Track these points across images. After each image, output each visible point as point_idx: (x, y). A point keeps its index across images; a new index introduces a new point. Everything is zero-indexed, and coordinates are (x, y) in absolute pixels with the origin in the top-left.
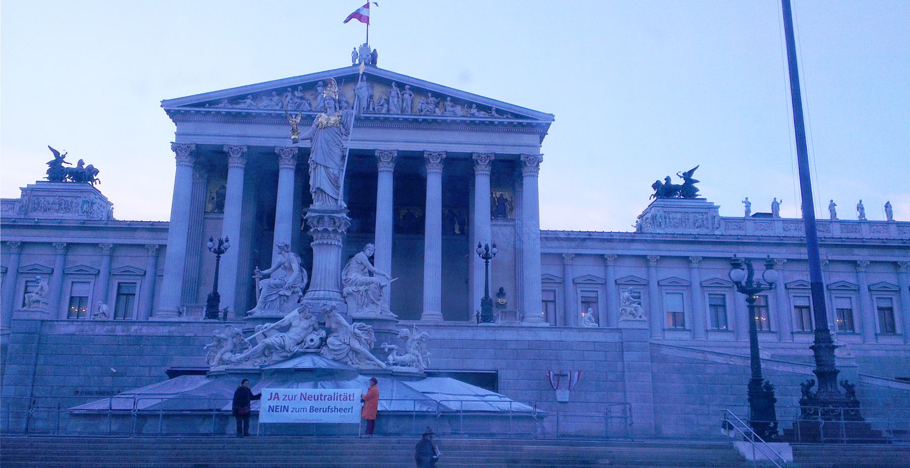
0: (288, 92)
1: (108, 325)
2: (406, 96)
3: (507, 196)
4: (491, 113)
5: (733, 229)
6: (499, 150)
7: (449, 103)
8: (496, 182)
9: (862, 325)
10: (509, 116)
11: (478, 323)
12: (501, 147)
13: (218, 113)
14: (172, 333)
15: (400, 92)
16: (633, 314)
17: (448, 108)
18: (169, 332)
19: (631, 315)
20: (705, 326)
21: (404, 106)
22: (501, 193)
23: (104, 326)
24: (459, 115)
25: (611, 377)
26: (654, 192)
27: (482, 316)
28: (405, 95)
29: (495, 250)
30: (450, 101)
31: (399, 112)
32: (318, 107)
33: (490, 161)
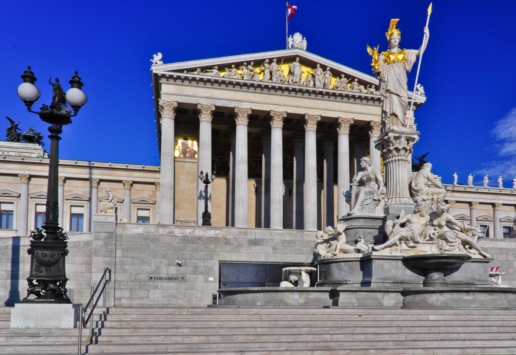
0: (244, 65)
1: (169, 228)
2: (327, 75)
7: (356, 83)
13: (194, 79)
14: (217, 235)
15: (324, 71)
17: (355, 87)
18: (215, 234)
21: (326, 83)
23: (166, 229)
24: (363, 92)
28: (326, 74)
30: (357, 82)
31: (322, 87)
32: (265, 80)
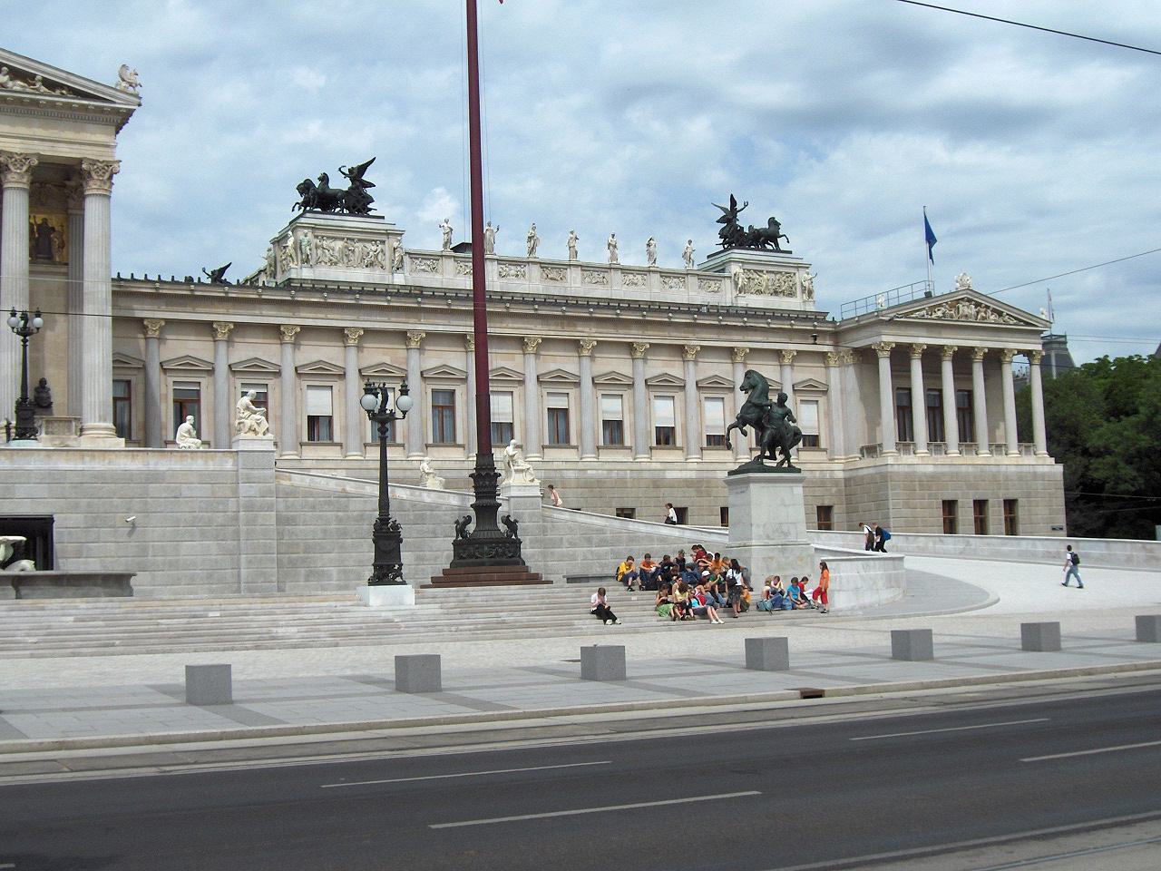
3: (54, 221)
4: (34, 85)
5: (423, 270)
6: (46, 148)
8: (38, 196)
9: (580, 436)
10: (64, 92)
11: (8, 440)
12: (51, 144)
16: (254, 430)
19: (251, 432)
20: (362, 437)
22: (43, 216)
25: (220, 518)
26: (301, 199)
27: (16, 428)
29: (38, 321)
33: (30, 166)
